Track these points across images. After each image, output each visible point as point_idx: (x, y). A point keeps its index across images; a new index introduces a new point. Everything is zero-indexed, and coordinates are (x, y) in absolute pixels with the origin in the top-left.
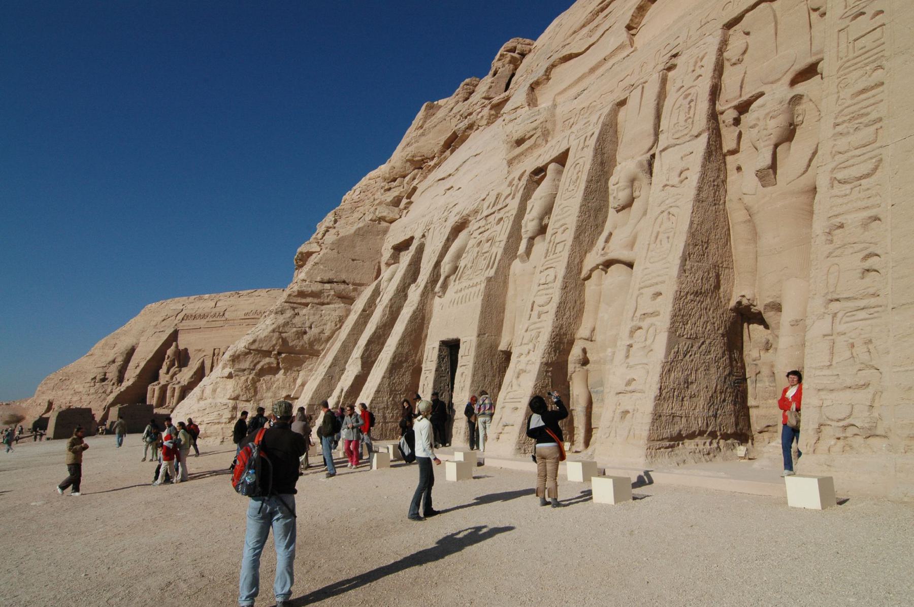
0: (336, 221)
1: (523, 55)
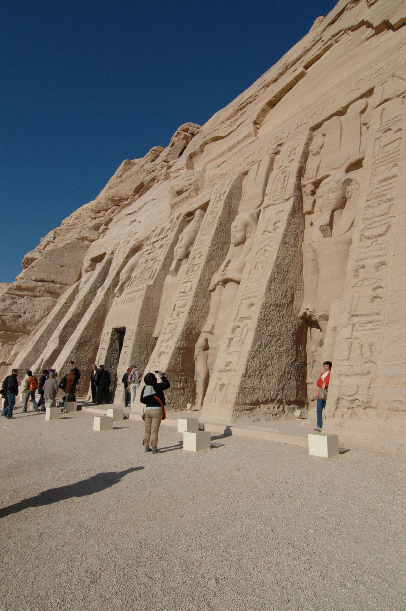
0: (55, 238)
1: (193, 135)
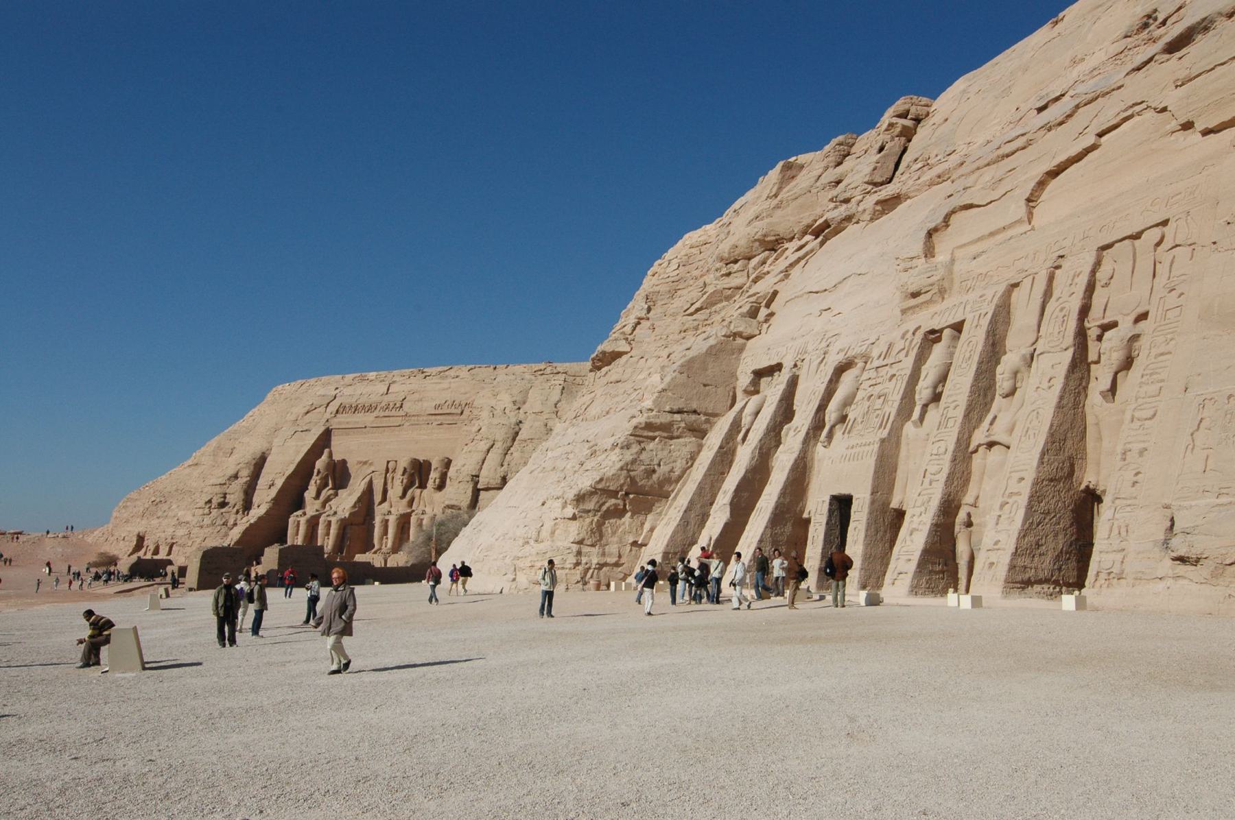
0: (649, 310)
1: (918, 120)
